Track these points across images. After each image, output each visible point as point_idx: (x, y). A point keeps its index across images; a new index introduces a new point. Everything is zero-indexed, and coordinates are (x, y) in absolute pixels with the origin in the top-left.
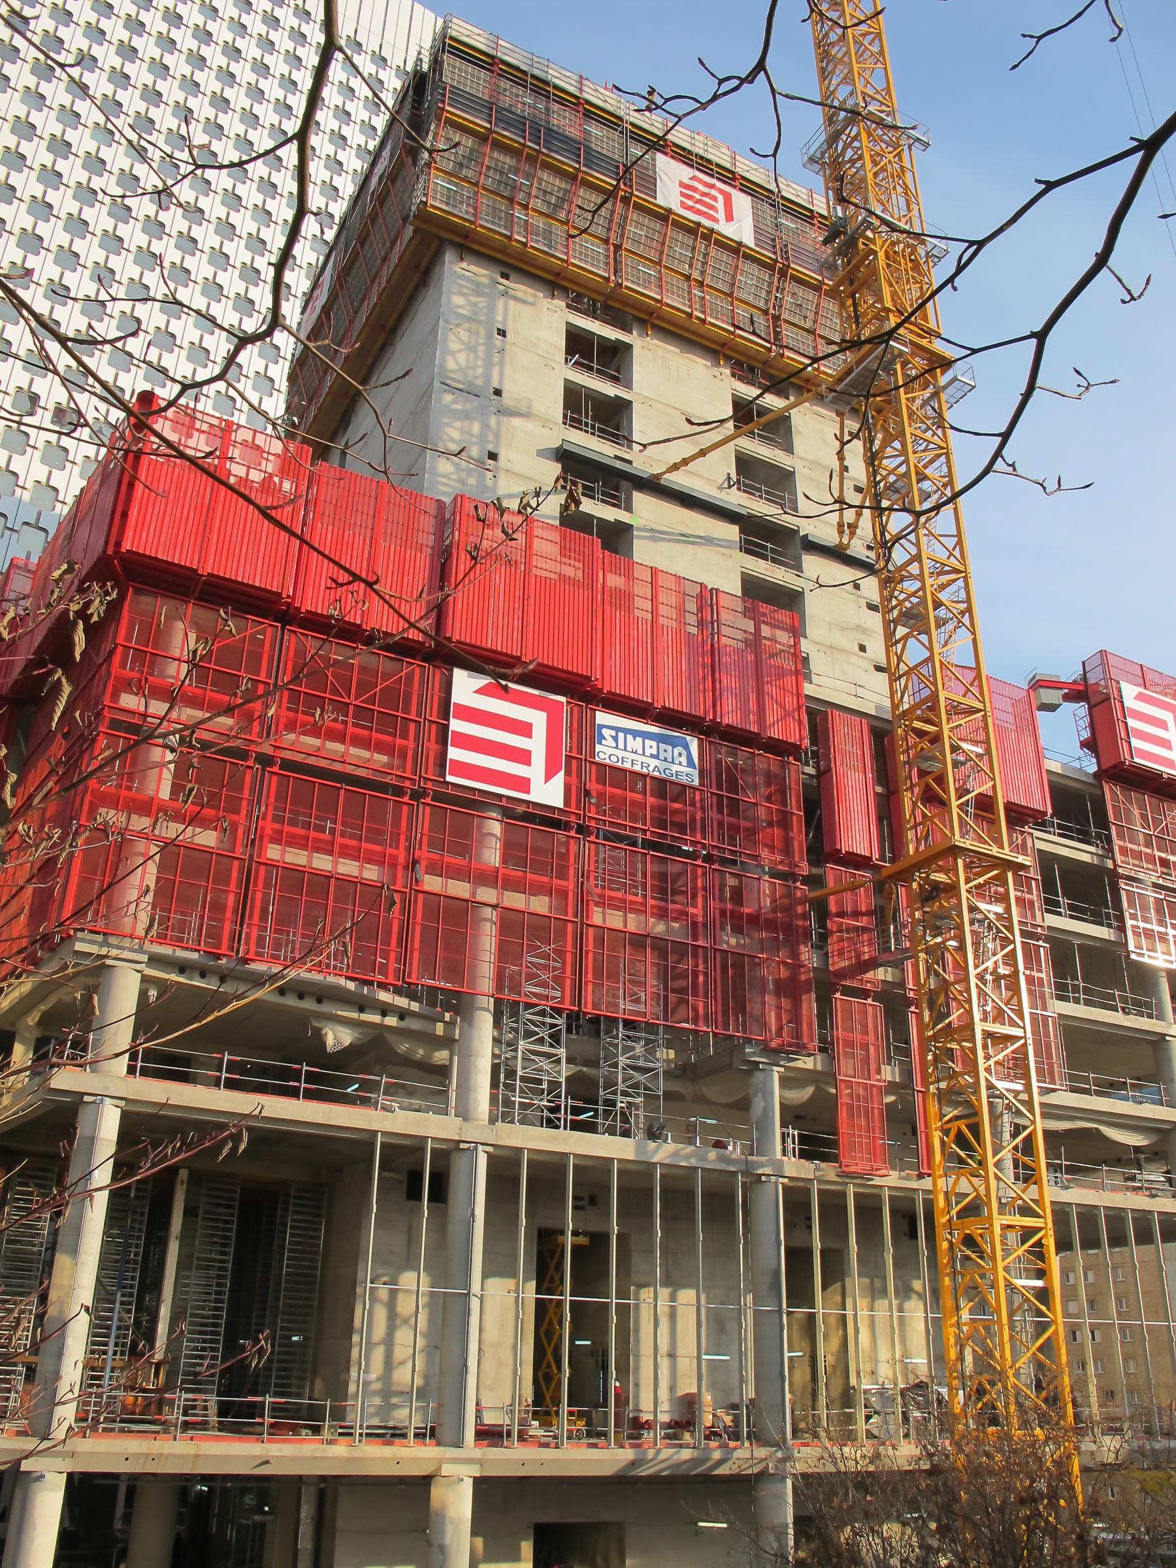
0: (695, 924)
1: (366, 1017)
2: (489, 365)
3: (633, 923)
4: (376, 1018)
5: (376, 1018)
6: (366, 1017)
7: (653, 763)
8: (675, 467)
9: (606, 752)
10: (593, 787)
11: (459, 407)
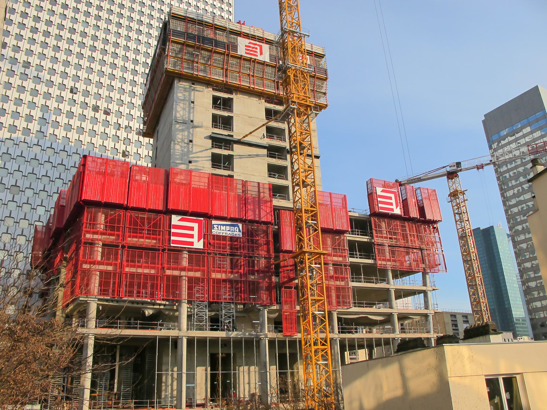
0: (241, 274)
1: (155, 307)
2: (189, 113)
3: (224, 276)
4: (158, 307)
5: (158, 307)
6: (155, 307)
7: (228, 232)
8: (244, 137)
11: (181, 128)
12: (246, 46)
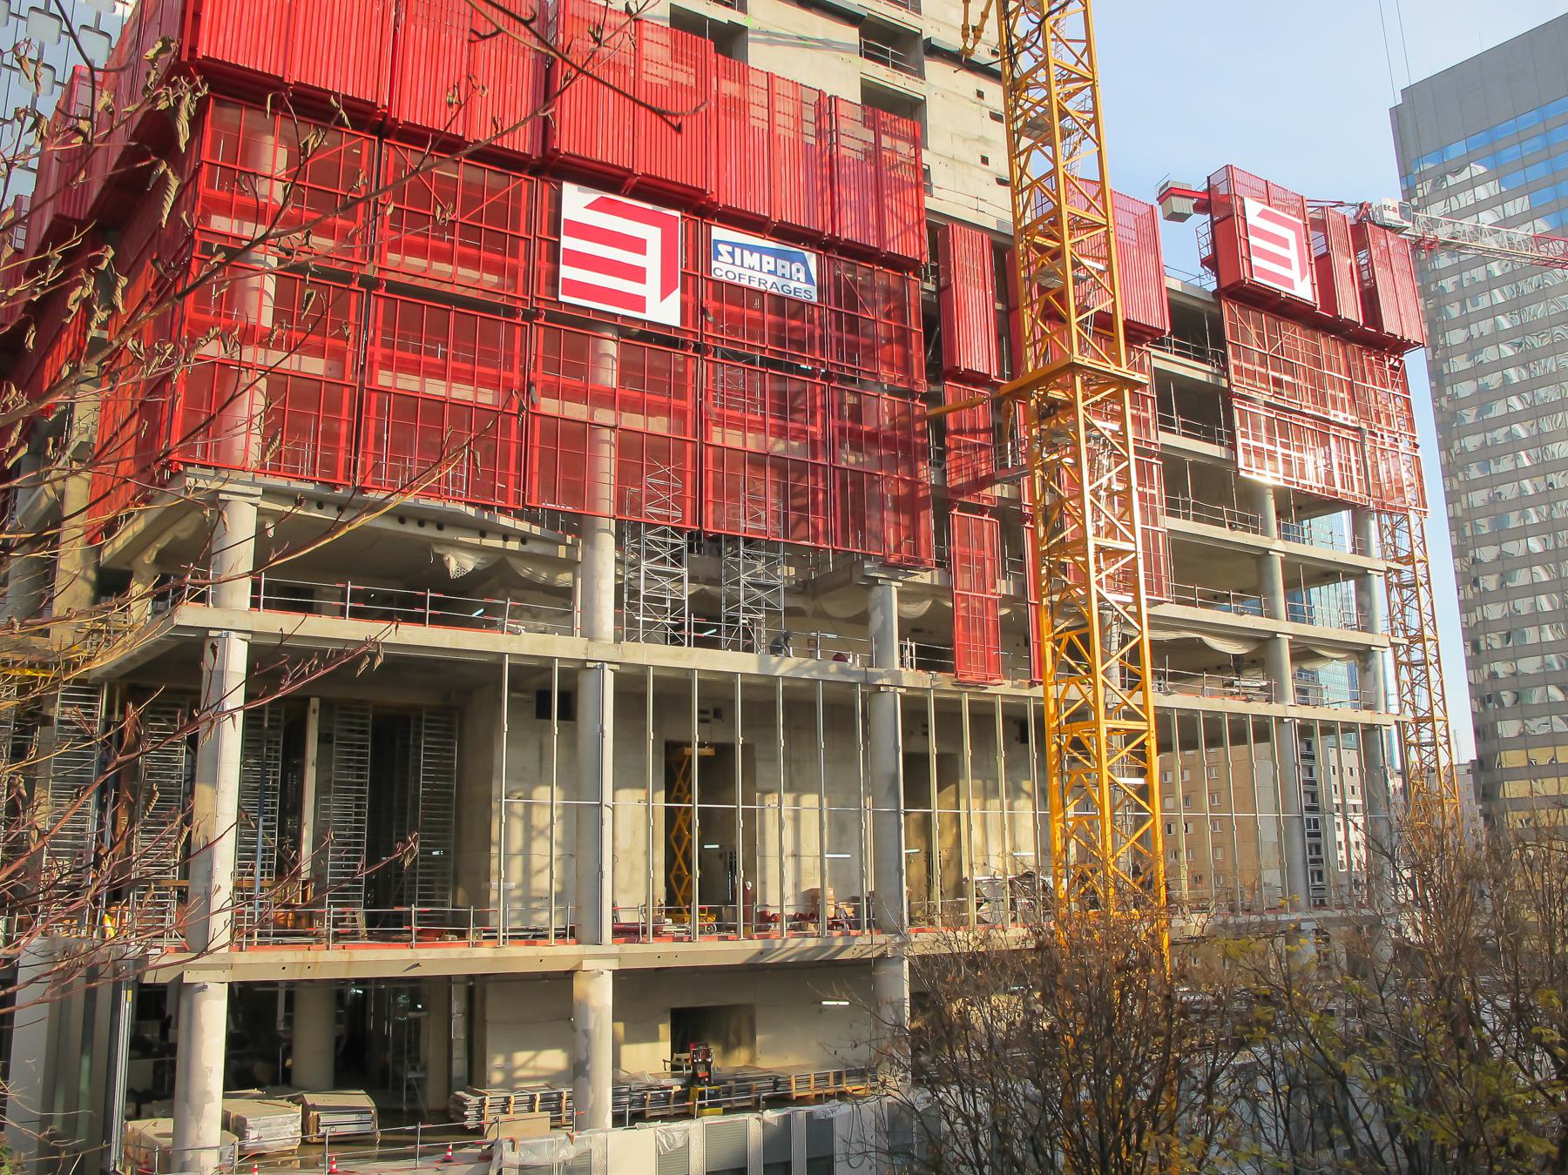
0: (814, 442)
1: (487, 542)
3: (753, 442)
6: (487, 542)
7: (771, 279)
10: (711, 305)
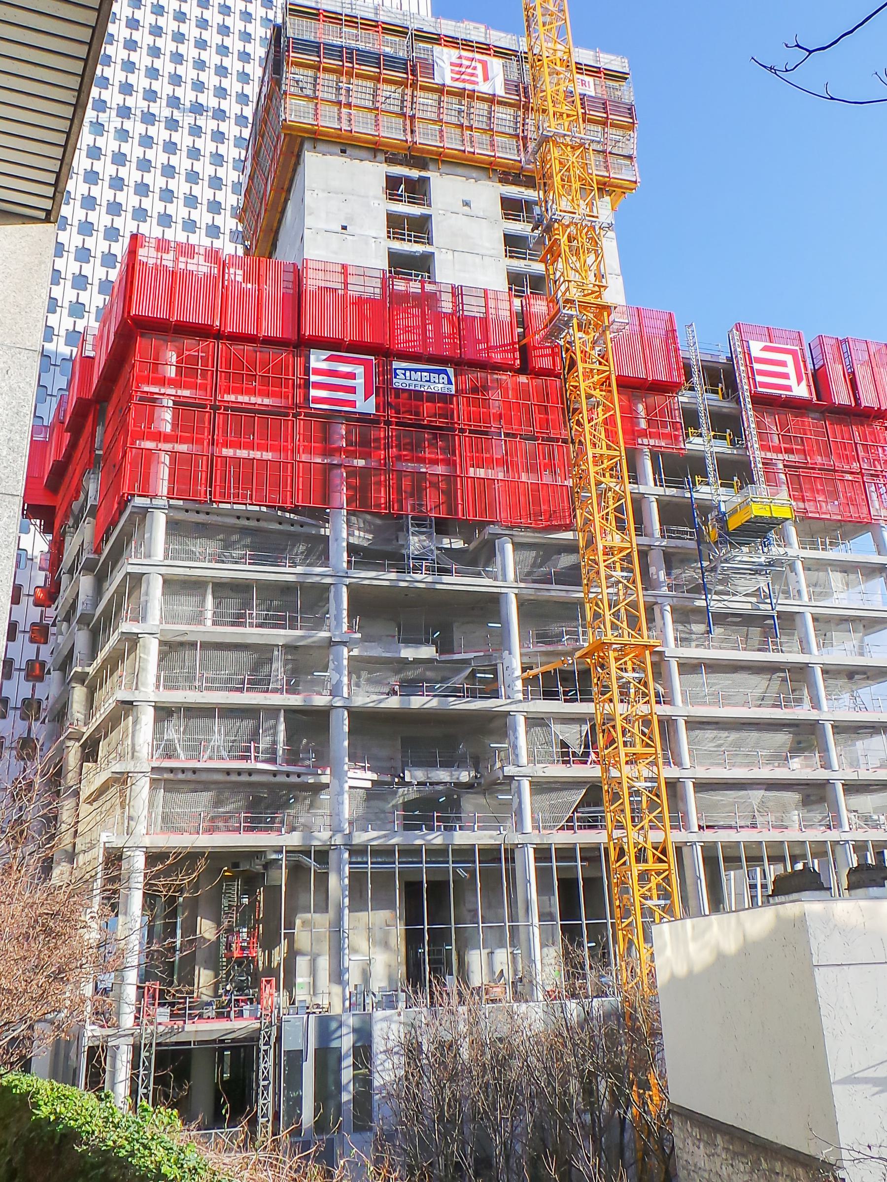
9: (399, 382)
12: (452, 64)
